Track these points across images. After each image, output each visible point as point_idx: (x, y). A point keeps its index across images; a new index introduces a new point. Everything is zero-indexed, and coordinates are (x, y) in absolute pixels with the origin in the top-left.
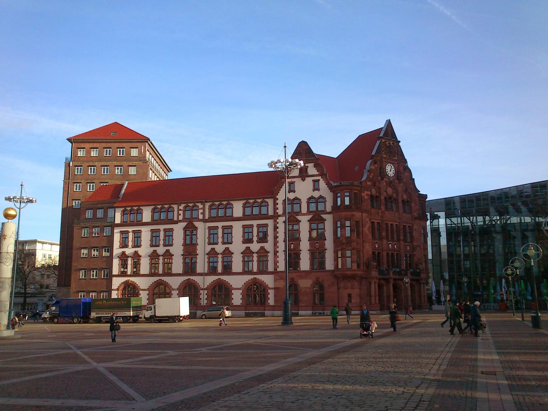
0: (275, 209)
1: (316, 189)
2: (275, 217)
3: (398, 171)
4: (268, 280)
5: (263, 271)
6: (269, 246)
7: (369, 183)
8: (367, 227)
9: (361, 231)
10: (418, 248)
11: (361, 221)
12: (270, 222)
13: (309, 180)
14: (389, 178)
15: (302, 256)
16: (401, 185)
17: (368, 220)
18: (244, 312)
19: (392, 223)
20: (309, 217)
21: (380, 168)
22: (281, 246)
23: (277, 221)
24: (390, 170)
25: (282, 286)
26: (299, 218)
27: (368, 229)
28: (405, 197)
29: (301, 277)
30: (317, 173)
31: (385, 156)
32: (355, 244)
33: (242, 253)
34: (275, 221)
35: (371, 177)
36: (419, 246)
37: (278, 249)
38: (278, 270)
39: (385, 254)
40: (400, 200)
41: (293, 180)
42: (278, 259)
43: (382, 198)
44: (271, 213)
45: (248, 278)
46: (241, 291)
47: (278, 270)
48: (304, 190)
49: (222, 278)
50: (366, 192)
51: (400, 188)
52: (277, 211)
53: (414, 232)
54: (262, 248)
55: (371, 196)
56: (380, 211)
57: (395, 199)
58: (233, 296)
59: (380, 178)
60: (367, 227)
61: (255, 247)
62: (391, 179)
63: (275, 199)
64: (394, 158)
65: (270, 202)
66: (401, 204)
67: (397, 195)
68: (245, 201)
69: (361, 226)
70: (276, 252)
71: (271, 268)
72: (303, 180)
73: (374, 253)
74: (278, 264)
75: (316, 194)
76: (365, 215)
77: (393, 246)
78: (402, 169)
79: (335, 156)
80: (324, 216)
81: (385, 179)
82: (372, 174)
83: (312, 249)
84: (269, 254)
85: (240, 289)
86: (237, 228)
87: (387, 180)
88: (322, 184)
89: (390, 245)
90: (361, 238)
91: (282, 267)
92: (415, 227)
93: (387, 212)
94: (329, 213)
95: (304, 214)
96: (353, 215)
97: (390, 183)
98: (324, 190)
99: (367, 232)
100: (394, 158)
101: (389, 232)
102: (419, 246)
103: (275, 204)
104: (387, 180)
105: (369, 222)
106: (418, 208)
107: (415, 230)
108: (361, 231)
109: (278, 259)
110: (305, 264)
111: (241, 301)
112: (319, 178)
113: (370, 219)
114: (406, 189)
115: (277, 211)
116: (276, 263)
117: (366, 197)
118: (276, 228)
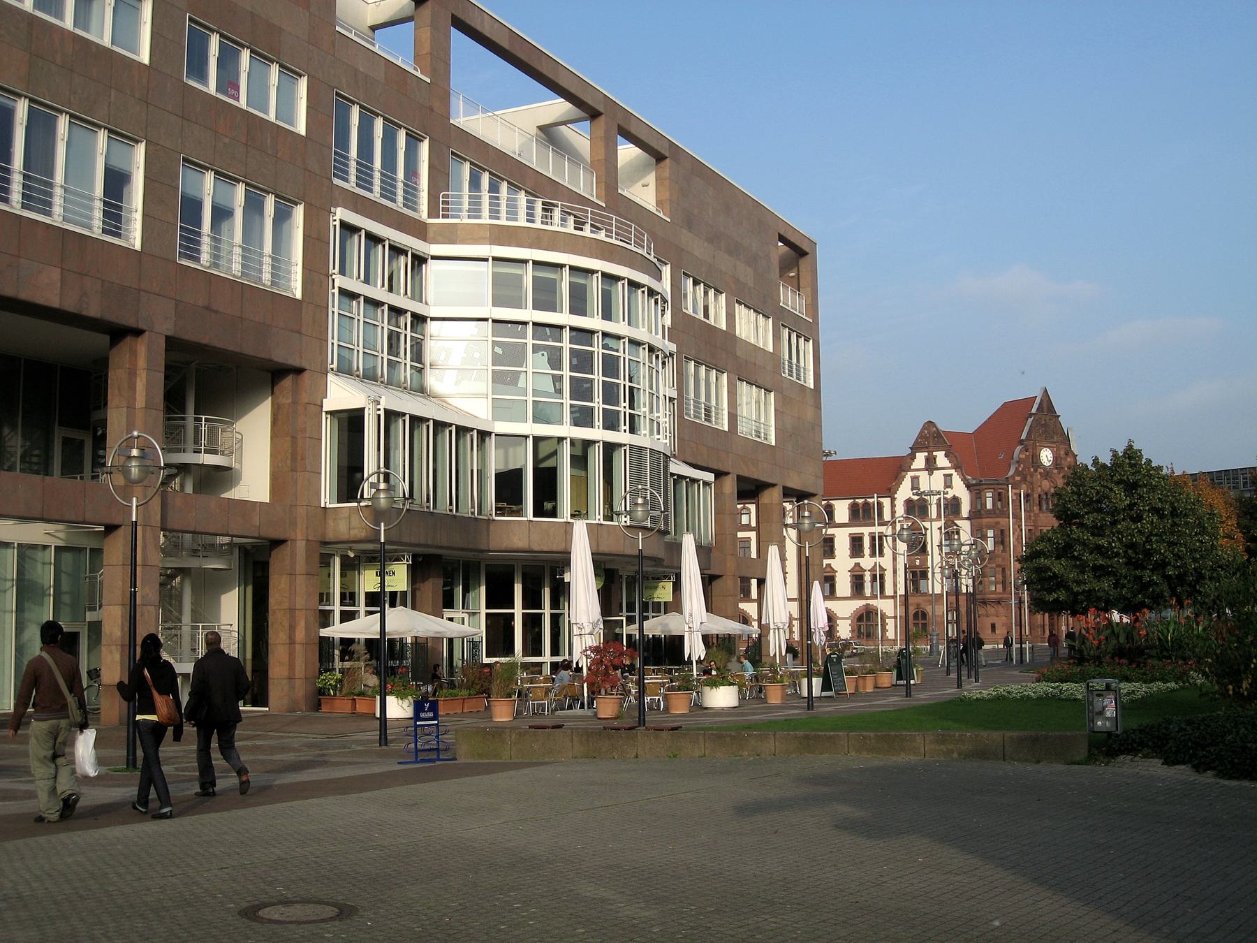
1: (948, 485)
7: (1018, 478)
13: (938, 476)
14: (1045, 468)
41: (917, 473)
45: (859, 604)
61: (867, 562)
63: (893, 500)
65: (886, 502)
70: (895, 572)
71: (889, 591)
79: (970, 429)
88: (957, 480)
94: (967, 519)
96: (998, 523)
97: (1047, 474)
98: (959, 489)
103: (893, 506)
112: (953, 471)
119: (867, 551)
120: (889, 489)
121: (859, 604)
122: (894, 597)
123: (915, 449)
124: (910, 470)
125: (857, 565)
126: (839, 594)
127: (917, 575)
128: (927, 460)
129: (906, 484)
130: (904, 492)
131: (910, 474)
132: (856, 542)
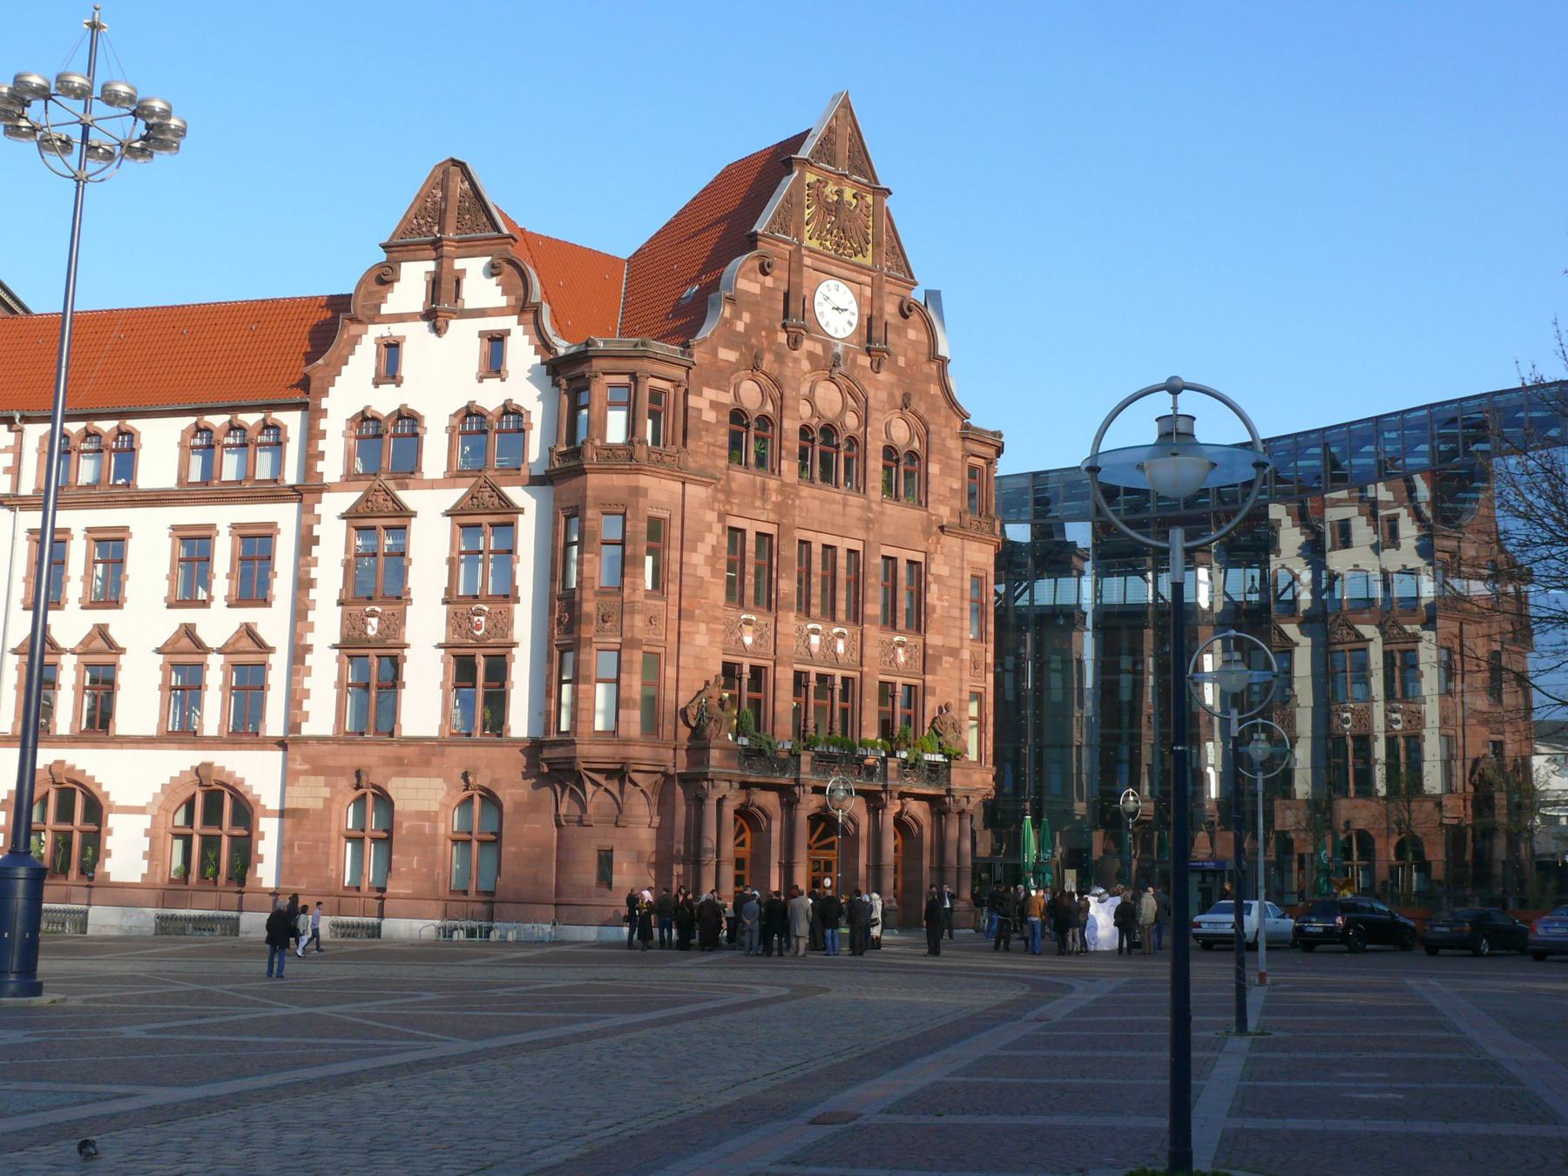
0: (311, 456)
1: (494, 365)
2: (307, 491)
3: (870, 320)
4: (258, 773)
5: (244, 730)
6: (273, 623)
7: (727, 355)
8: (705, 548)
9: (675, 568)
10: (947, 661)
11: (677, 521)
12: (284, 515)
14: (827, 343)
15: (408, 672)
16: (883, 376)
17: (712, 516)
18: (152, 912)
19: (829, 540)
20: (454, 496)
21: (787, 296)
22: (327, 623)
23: (318, 509)
24: (836, 308)
25: (319, 805)
26: (408, 497)
27: (711, 560)
28: (901, 434)
29: (402, 767)
30: (502, 301)
31: (814, 244)
32: (639, 621)
33: (159, 651)
34: (306, 511)
35: (740, 327)
36: (954, 653)
37: (310, 639)
38: (306, 730)
39: (785, 676)
40: (875, 446)
41: (396, 330)
42: (308, 683)
43: (791, 426)
44: (291, 476)
46: (145, 821)
47: (306, 730)
48: (442, 377)
49: (69, 762)
50: (710, 394)
51: (881, 387)
52: (321, 466)
53: (934, 588)
54: (249, 631)
55: (737, 416)
56: (773, 484)
57: (852, 440)
58: (110, 843)
59: (782, 337)
60: (705, 548)
61: (217, 623)
62: (839, 349)
64: (859, 259)
66: (875, 464)
67: (865, 421)
68: (193, 420)
69: (676, 543)
70: (299, 653)
72: (438, 330)
73: (730, 670)
74: (306, 705)
75: (491, 396)
76: (696, 492)
77: (828, 644)
78: (891, 309)
80: (517, 494)
81: (807, 345)
82: (746, 317)
83: (457, 639)
84: (272, 659)
85: (141, 810)
86: (150, 539)
87: (819, 349)
89: (815, 640)
90: (673, 599)
91: (321, 719)
92: (938, 568)
93: (806, 491)
95: (433, 484)
96: (636, 492)
97: (831, 364)
99: (705, 572)
100: (859, 259)
101: (816, 581)
102: (954, 653)
103: (312, 434)
104: (819, 349)
105: (718, 528)
106: (957, 485)
107: (939, 579)
108: (675, 568)
109: (308, 683)
110: (423, 705)
111: (143, 867)
112: (509, 322)
113: (722, 517)
114: (907, 399)
115: (321, 466)
116: (295, 699)
117: (710, 416)
118: (307, 541)
119: (221, 585)
120: (305, 384)
121: (183, 760)
122: (282, 744)
123: (399, 249)
124: (376, 317)
125: (188, 631)
126: (123, 724)
127: (375, 672)
128: (435, 283)
129: (364, 358)
130: (352, 389)
131: (376, 331)
132: (194, 550)
